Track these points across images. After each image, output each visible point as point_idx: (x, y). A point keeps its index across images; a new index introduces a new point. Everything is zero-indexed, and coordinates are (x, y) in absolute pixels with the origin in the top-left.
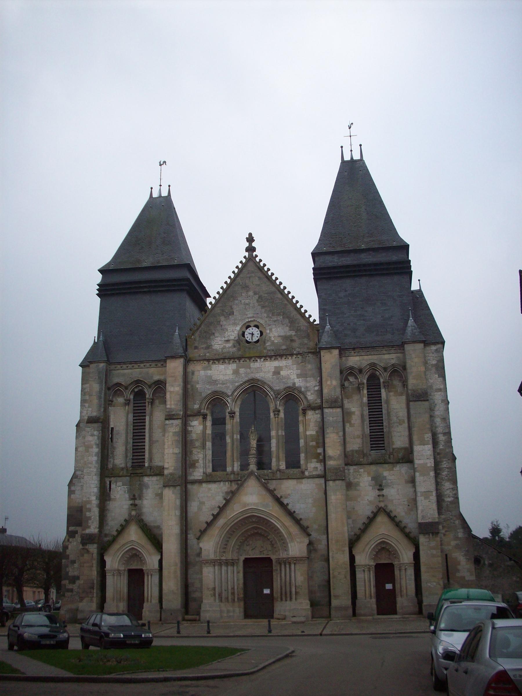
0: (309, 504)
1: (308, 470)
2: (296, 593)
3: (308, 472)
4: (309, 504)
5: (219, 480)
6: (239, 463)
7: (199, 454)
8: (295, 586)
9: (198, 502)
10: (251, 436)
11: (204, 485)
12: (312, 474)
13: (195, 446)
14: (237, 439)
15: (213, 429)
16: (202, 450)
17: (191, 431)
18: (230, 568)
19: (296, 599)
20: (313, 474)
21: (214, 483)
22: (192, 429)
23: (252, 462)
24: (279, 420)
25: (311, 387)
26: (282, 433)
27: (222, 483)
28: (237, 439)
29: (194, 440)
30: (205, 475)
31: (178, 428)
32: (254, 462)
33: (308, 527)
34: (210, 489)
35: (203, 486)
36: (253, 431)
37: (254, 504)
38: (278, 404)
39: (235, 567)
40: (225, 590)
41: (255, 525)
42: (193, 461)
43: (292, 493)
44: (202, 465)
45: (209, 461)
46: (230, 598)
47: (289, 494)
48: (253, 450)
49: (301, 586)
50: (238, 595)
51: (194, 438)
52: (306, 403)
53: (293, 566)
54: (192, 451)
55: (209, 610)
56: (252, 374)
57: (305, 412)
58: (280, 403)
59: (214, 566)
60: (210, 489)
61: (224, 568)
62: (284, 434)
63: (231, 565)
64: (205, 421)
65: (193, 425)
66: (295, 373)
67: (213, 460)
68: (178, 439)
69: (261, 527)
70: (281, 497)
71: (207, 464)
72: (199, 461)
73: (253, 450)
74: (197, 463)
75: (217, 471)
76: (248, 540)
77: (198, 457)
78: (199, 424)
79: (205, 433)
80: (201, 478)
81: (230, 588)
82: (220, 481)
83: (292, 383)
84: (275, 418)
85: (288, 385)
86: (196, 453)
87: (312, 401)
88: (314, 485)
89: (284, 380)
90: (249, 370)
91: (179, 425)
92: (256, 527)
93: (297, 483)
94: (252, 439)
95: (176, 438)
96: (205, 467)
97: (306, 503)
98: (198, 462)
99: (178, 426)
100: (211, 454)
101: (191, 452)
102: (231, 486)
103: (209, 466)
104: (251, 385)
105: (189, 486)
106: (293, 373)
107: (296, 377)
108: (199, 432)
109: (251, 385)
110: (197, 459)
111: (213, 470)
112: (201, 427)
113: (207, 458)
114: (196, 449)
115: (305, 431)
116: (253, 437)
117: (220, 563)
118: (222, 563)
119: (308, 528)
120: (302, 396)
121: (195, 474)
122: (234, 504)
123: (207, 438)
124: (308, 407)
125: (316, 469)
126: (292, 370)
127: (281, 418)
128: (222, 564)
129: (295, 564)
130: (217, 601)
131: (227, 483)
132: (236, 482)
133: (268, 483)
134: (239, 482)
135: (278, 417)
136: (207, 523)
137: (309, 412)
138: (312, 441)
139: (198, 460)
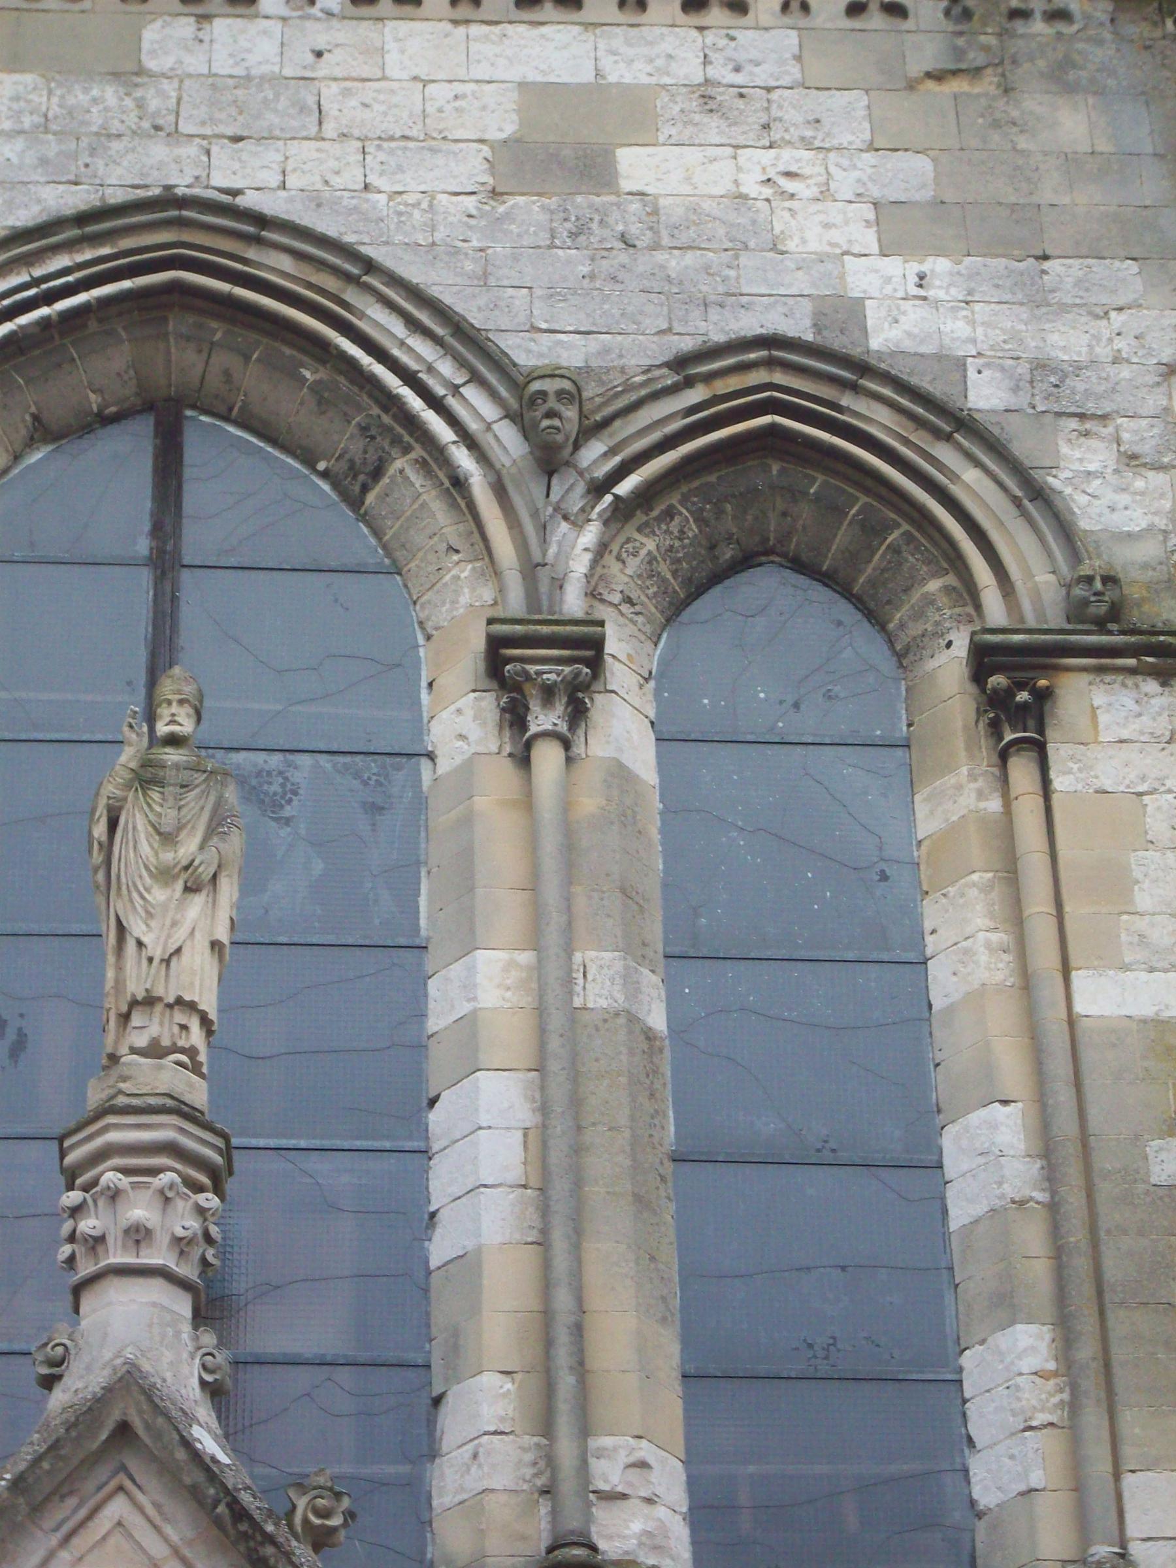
10: (135, 820)
23: (138, 1235)
24: (589, 804)
25: (1125, 372)
26: (632, 987)
32: (181, 1245)
36: (172, 756)
38: (580, 565)
48: (155, 1051)
52: (1044, 578)
56: (158, 151)
57: (1044, 696)
58: (601, 550)
62: (658, 1019)
66: (844, 183)
73: (155, 1051)
83: (807, 306)
84: (523, 760)
85: (749, 324)
87: (1149, 550)
89: (675, 263)
90: (110, 94)
94: (164, 875)
104: (127, 284)
106: (825, 194)
107: (869, 239)
109: (127, 284)
115: (1045, 957)
116: (168, 838)
120: (971, 475)
124: (1101, 625)
126: (807, 144)
135: (567, 745)
137: (1099, 697)
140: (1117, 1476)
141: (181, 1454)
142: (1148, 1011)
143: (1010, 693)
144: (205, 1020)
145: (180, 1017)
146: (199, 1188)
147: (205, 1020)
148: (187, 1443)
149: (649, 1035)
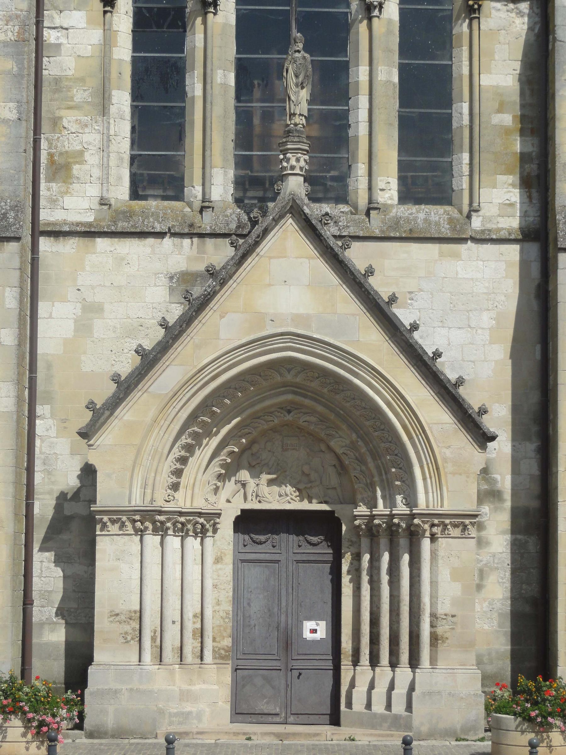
0: (480, 331)
1: (480, 213)
2: (435, 639)
3: (481, 219)
4: (480, 331)
5: (158, 228)
6: (231, 173)
7: (87, 130)
8: (433, 616)
9: (79, 306)
11: (101, 243)
12: (494, 226)
13: (71, 103)
14: (224, 85)
15: (137, 46)
16: (99, 119)
17: (58, 46)
18: (193, 543)
19: (433, 661)
20: (500, 226)
21: (139, 238)
22: (63, 40)
26: (390, 73)
27: (168, 241)
28: (224, 85)
29: (67, 78)
30: (106, 207)
31: (17, 28)
33: (483, 411)
34: (121, 261)
35: (98, 250)
37: (297, 318)
39: (208, 541)
40: (174, 622)
41: (290, 397)
42: (61, 154)
43: (421, 290)
44: (96, 173)
45: (122, 159)
46: (188, 650)
47: (410, 293)
49: (453, 616)
50: (214, 640)
51: (70, 73)
53: (426, 543)
54: (61, 118)
55: (116, 692)
57: (480, 6)
59: (141, 533)
60: (123, 259)
61: (173, 542)
63: (196, 536)
64: (111, 12)
65: (65, 26)
67: (133, 159)
68: (15, 69)
69: (307, 402)
70: (393, 299)
71: (113, 172)
72: (87, 156)
74: (77, 163)
75: (144, 198)
76: (255, 448)
77: (81, 143)
78: (90, 21)
79: (110, 59)
80: (90, 218)
81: (189, 614)
82: (160, 235)
86: (74, 127)
88: (503, 266)
91: (17, 17)
92: (292, 402)
93: (441, 254)
95: (9, 65)
96: (104, 180)
97: (470, 326)
98: (82, 162)
99: (16, 22)
100: (128, 135)
101: (56, 122)
102: (201, 250)
103: (120, 178)
105: (44, 244)
108: (88, 51)
110: (79, 148)
111: (135, 195)
112: (96, 35)
113: (113, 147)
114: (76, 112)
117: (162, 523)
118: (169, 525)
119: (486, 412)
121: (68, 201)
122: (222, 317)
123: (114, 74)
125: (509, 210)
127: (390, 21)
128: (168, 529)
129: (433, 538)
130: (147, 656)
131: (187, 242)
132: (227, 241)
133: (345, 247)
134: (241, 241)
136: (116, 378)
138: (500, 111)
139: (81, 153)
140: (479, 188)
141: (302, 213)
142: (495, 84)
143: (473, 5)
144: (305, 117)
145: (301, 117)
146: (305, 154)
147: (305, 117)
148: (303, 211)
149: (394, 84)
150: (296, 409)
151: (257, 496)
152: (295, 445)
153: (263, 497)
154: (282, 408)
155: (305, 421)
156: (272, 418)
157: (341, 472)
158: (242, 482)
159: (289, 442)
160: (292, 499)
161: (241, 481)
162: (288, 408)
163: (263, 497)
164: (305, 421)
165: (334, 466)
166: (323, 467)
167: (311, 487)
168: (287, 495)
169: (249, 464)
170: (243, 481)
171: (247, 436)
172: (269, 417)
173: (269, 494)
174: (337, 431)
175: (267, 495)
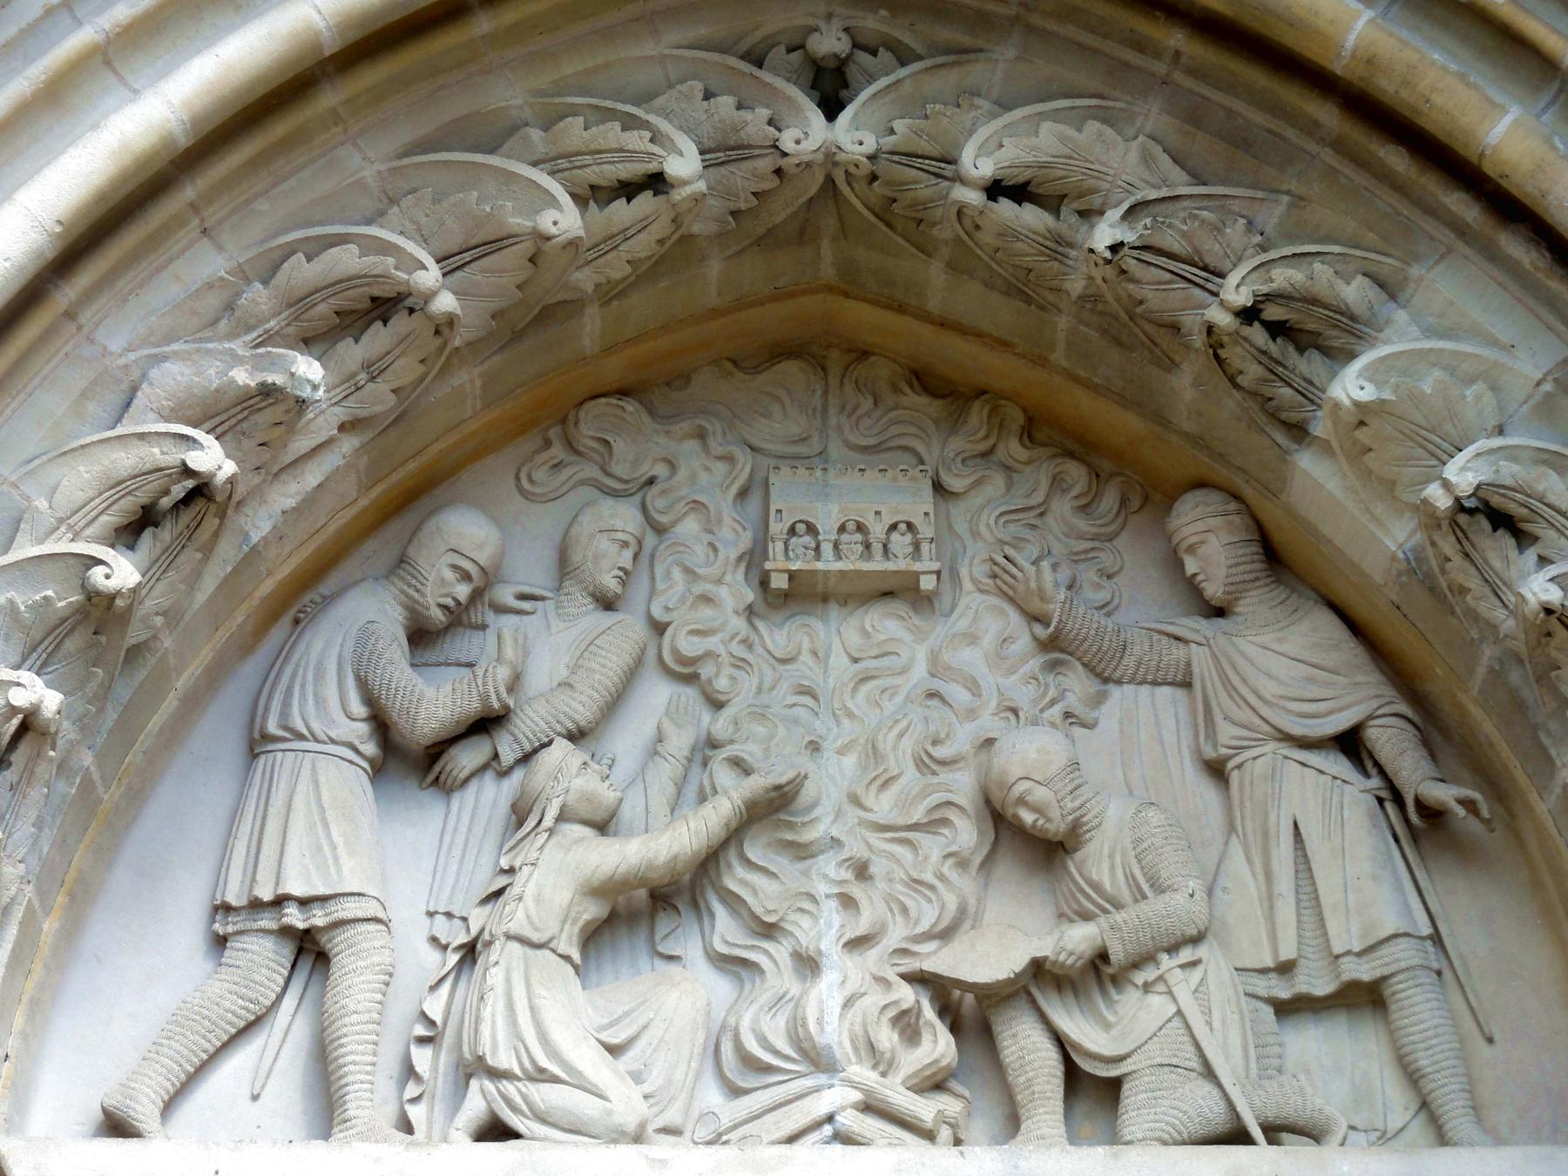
150: (903, 56)
151: (474, 1068)
152: (901, 542)
153: (541, 1076)
154: (757, 59)
155: (1020, 192)
156: (637, 140)
157: (1443, 794)
158: (294, 917)
159: (828, 518)
160: (871, 1107)
161: (280, 901)
162: (829, 43)
163: (541, 1076)
164: (1020, 192)
165: (1350, 744)
166: (1217, 770)
167: (1103, 956)
168: (818, 1060)
169: (381, 724)
170: (304, 903)
171: (353, 352)
172: (612, 134)
173: (614, 1050)
174: (1388, 264)
175: (590, 1061)
